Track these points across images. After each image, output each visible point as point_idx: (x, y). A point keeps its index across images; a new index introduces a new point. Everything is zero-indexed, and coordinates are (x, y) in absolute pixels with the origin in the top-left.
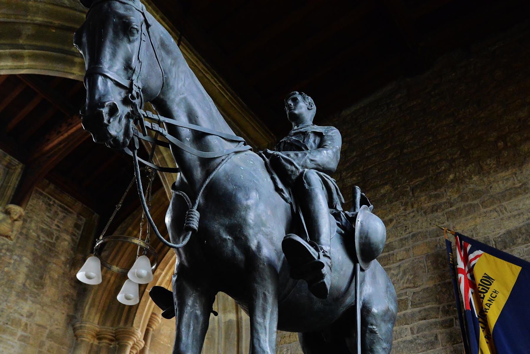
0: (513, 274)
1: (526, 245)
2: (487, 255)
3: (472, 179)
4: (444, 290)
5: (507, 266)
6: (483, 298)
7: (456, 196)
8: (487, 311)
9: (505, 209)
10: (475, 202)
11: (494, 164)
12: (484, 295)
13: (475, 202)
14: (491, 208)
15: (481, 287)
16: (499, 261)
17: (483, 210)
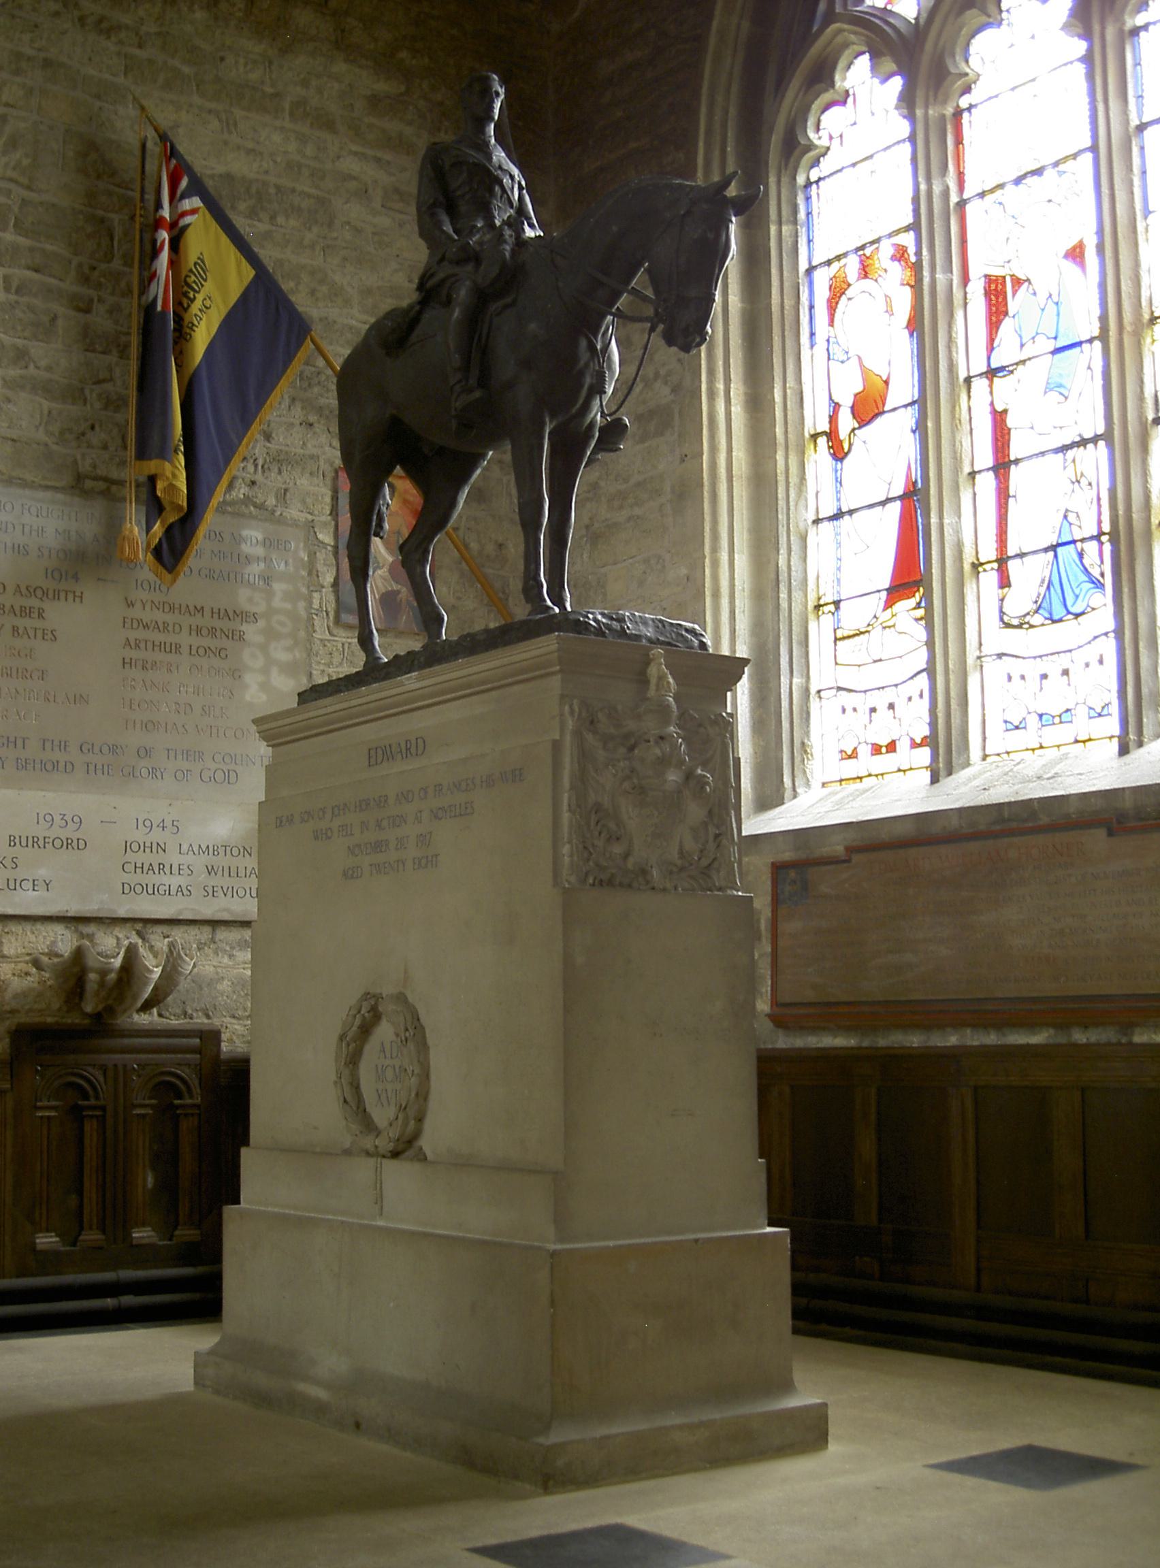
0: (241, 281)
1: (249, 221)
2: (208, 215)
3: (194, 12)
4: (89, 229)
5: (233, 257)
6: (193, 300)
7: (153, 29)
8: (195, 328)
9: (235, 125)
10: (186, 70)
11: (240, 10)
12: (194, 295)
13: (186, 70)
14: (213, 105)
15: (193, 278)
16: (225, 240)
17: (197, 100)
